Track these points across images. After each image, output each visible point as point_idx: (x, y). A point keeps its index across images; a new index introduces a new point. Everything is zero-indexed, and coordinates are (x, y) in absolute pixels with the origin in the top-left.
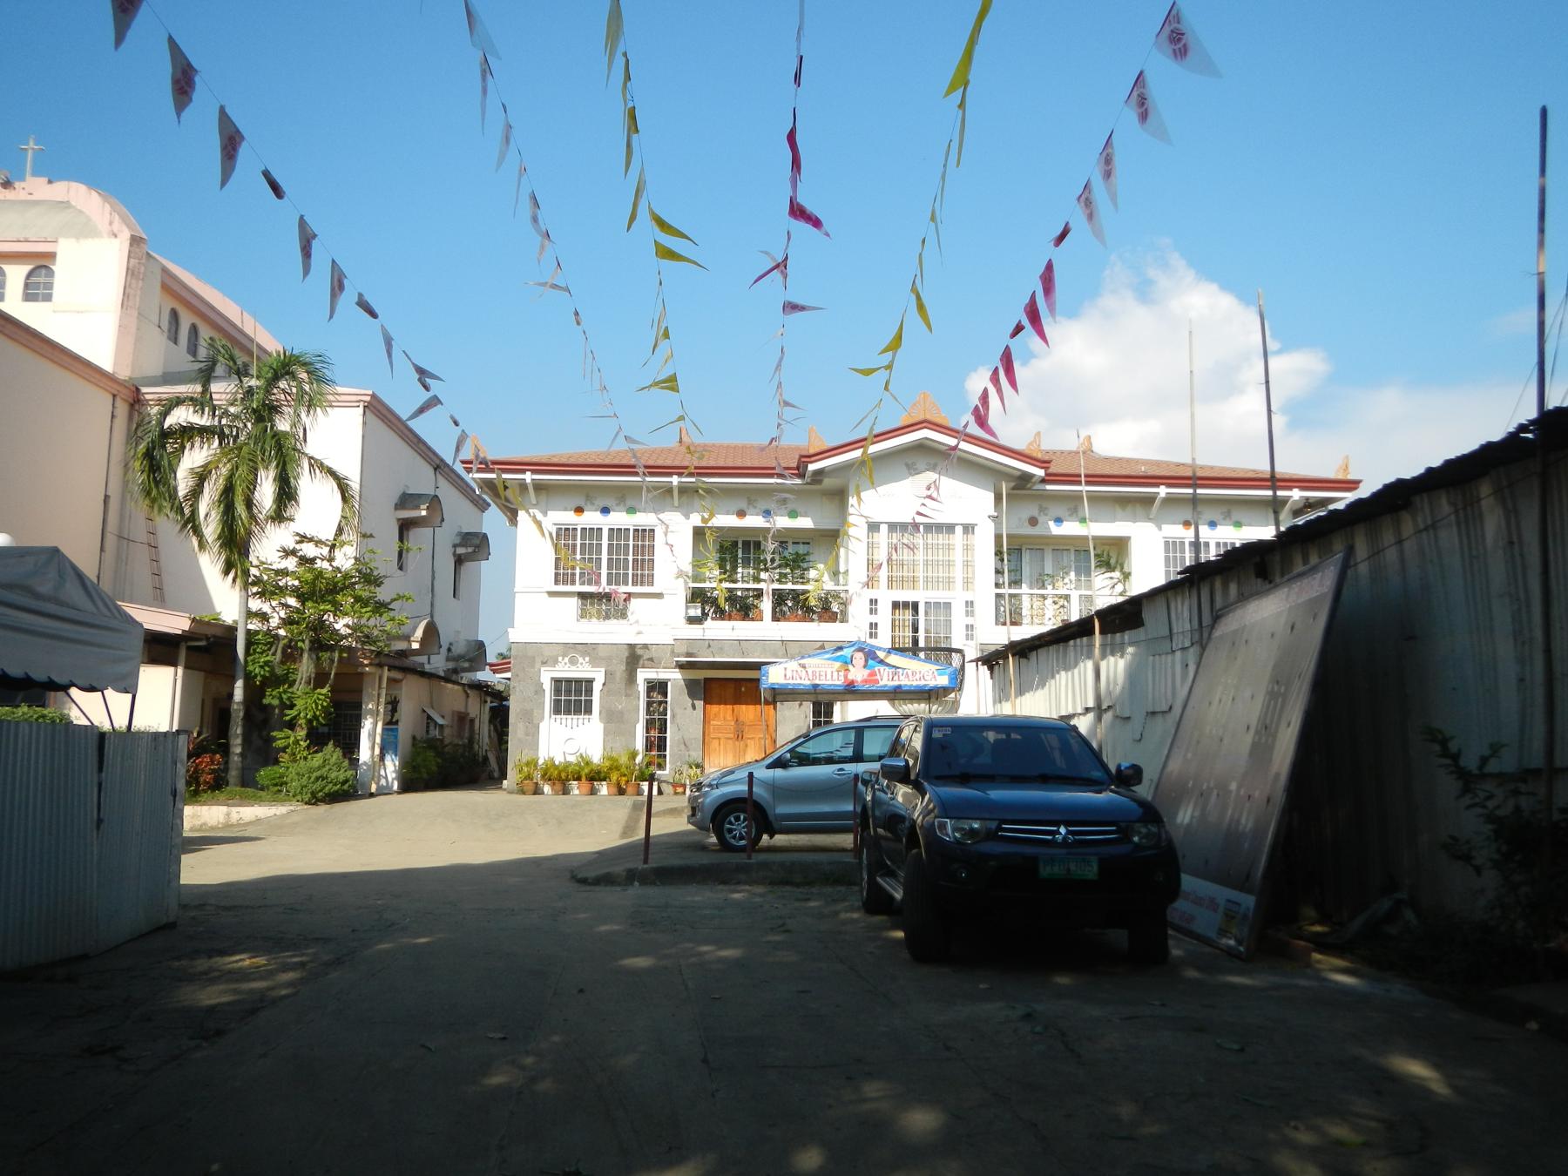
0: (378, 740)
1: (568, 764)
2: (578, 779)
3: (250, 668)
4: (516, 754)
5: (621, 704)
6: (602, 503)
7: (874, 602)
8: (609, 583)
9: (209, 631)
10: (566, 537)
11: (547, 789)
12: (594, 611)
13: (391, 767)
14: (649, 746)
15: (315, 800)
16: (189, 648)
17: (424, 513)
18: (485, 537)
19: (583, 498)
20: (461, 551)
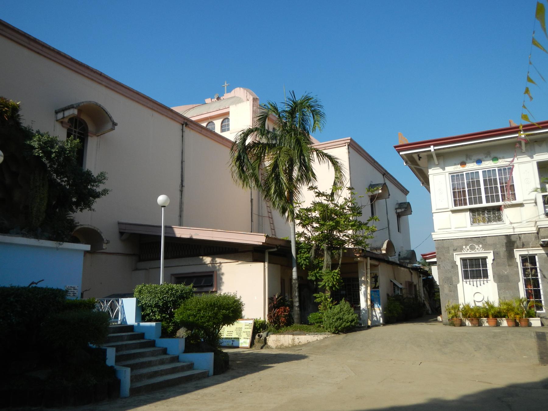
0: (369, 297)
1: (478, 309)
2: (487, 317)
3: (299, 261)
4: (445, 303)
5: (506, 271)
6: (476, 157)
8: (488, 201)
9: (278, 243)
10: (458, 180)
11: (468, 323)
12: (481, 218)
13: (378, 311)
14: (529, 294)
15: (337, 331)
16: (270, 253)
17: (380, 191)
18: (409, 204)
19: (464, 156)
20: (399, 211)
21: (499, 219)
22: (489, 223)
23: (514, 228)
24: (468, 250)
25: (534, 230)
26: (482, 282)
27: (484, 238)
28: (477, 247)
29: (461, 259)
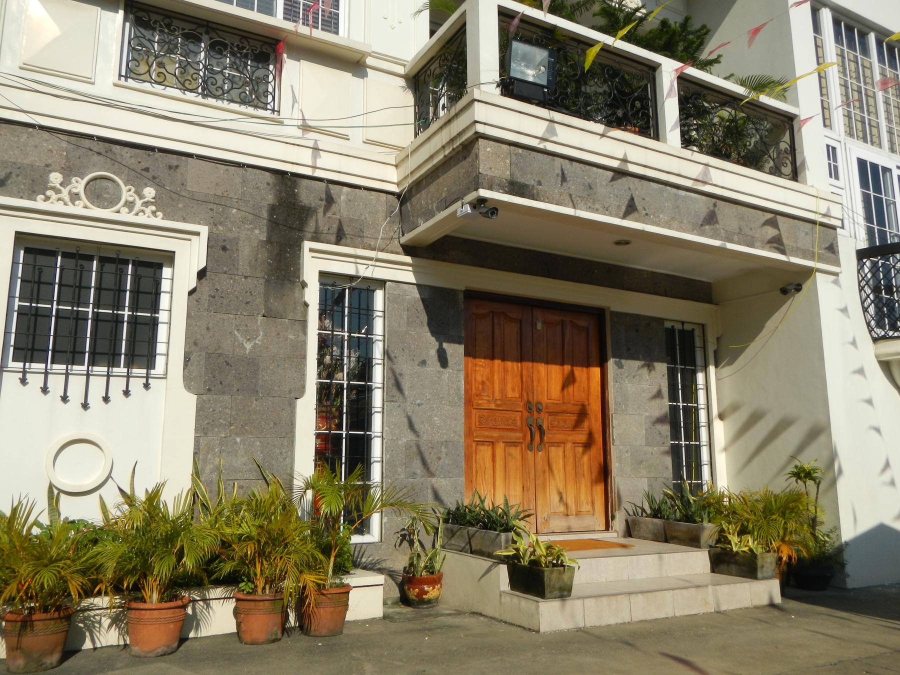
5: (250, 339)
7: (832, 152)
21: (256, 95)
22: (211, 101)
23: (316, 149)
24: (75, 197)
25: (391, 178)
26: (117, 385)
27: (174, 160)
28: (127, 193)
29: (21, 238)
